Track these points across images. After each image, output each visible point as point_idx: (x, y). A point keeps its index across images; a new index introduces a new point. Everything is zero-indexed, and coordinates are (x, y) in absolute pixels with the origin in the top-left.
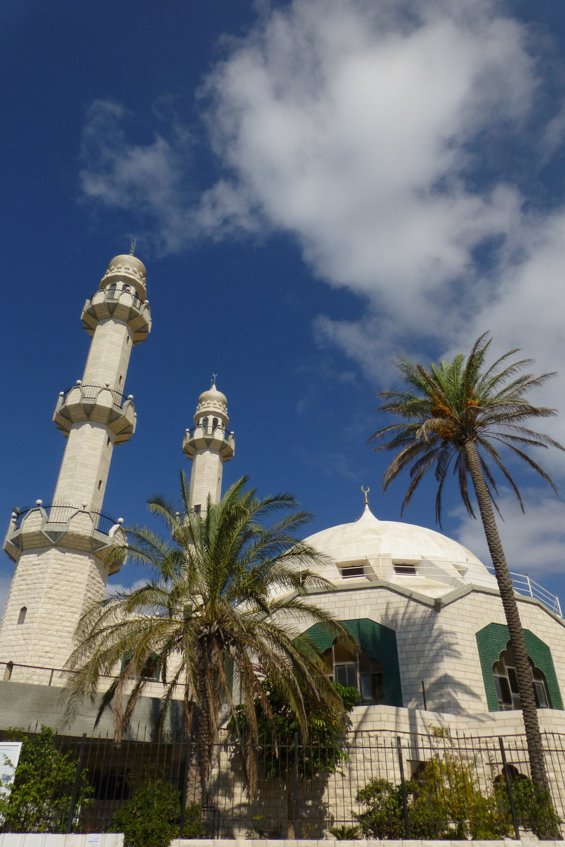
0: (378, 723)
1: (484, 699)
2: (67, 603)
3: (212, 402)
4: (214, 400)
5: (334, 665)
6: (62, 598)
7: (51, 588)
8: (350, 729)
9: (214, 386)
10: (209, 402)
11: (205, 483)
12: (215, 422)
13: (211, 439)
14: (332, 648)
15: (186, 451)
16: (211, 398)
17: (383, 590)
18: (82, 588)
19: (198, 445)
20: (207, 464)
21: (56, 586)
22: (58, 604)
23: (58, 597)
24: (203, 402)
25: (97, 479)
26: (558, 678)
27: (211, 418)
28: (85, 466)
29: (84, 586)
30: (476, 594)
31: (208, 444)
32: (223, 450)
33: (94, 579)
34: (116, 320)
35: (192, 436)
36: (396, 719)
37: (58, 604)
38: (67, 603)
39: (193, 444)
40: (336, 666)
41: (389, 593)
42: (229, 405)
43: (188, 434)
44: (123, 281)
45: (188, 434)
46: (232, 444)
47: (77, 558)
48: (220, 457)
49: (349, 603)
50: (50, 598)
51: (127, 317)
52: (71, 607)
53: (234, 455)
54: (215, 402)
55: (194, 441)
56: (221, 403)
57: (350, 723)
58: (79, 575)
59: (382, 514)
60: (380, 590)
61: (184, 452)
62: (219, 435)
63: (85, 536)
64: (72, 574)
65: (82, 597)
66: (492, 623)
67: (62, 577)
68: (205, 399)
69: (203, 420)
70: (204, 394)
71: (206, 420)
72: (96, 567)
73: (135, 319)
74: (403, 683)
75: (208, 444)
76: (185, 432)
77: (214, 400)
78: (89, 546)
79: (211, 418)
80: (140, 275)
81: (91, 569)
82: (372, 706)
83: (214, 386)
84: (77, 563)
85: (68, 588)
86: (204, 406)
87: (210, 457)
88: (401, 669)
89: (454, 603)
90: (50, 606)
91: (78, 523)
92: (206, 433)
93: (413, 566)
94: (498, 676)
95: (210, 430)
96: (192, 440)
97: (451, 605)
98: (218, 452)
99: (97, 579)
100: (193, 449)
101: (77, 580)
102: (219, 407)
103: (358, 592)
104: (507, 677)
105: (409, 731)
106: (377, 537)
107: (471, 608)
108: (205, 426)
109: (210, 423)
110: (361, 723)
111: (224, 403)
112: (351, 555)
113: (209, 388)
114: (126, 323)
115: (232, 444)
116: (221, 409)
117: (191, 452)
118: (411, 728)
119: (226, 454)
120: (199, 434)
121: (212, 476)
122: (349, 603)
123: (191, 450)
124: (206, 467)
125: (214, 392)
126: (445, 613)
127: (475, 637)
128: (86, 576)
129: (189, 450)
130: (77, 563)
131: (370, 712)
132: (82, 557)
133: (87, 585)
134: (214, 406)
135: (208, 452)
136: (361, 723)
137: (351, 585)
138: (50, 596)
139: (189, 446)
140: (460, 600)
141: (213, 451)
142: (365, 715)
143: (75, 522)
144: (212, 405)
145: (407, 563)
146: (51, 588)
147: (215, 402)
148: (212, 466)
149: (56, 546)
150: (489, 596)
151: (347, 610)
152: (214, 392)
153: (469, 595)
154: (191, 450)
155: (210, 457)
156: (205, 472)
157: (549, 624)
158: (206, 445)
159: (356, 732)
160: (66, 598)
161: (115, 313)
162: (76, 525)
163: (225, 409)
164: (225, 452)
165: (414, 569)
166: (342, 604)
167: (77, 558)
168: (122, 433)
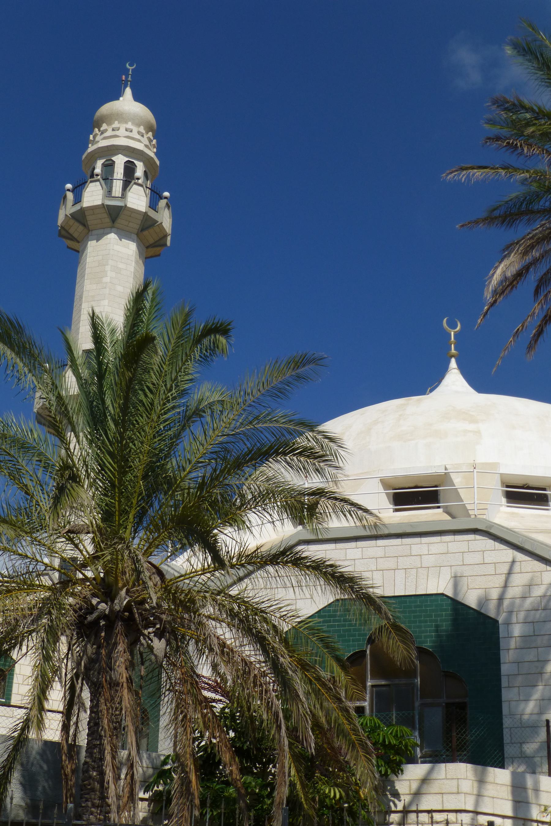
0: (453, 796)
3: (123, 127)
4: (126, 122)
5: (369, 684)
8: (396, 805)
9: (128, 91)
10: (116, 124)
11: (106, 302)
12: (129, 169)
13: (121, 207)
14: (366, 651)
15: (64, 233)
16: (121, 117)
17: (478, 537)
19: (91, 220)
20: (110, 262)
24: (104, 126)
27: (120, 161)
31: (114, 217)
32: (146, 233)
35: (78, 199)
39: (80, 216)
40: (373, 686)
41: (490, 543)
42: (161, 132)
43: (70, 196)
45: (70, 196)
46: (165, 218)
48: (138, 246)
49: (404, 562)
53: (168, 244)
54: (130, 125)
55: (82, 211)
56: (142, 129)
57: (396, 795)
59: (481, 382)
60: (471, 537)
61: (60, 235)
62: (138, 199)
68: (108, 119)
69: (104, 165)
70: (107, 108)
71: (109, 166)
74: (507, 722)
75: (114, 217)
76: (65, 191)
77: (126, 122)
79: (120, 161)
82: (443, 765)
83: (128, 91)
86: (106, 135)
87: (117, 248)
88: (506, 695)
92: (109, 193)
93: (544, 489)
95: (117, 187)
96: (77, 207)
98: (135, 237)
100: (81, 228)
102: (138, 137)
103: (425, 540)
105: (510, 813)
106: (471, 427)
108: (107, 178)
109: (119, 171)
110: (417, 794)
111: (149, 128)
112: (415, 463)
113: (117, 95)
115: (165, 218)
116: (143, 143)
117: (76, 235)
118: (516, 808)
119: (151, 241)
120: (93, 195)
121: (120, 288)
122: (404, 562)
123: (76, 229)
124: (108, 268)
125: (127, 104)
129: (71, 231)
131: (434, 775)
134: (128, 134)
135: (112, 236)
136: (417, 794)
137: (411, 525)
139: (72, 222)
141: (123, 234)
142: (425, 780)
144: (122, 132)
145: (531, 484)
147: (130, 125)
148: (121, 266)
151: (400, 575)
152: (127, 104)
154: (76, 229)
155: (117, 248)
156: (107, 280)
158: (108, 220)
159: (405, 812)
163: (150, 141)
164: (151, 236)
165: (546, 496)
166: (390, 563)
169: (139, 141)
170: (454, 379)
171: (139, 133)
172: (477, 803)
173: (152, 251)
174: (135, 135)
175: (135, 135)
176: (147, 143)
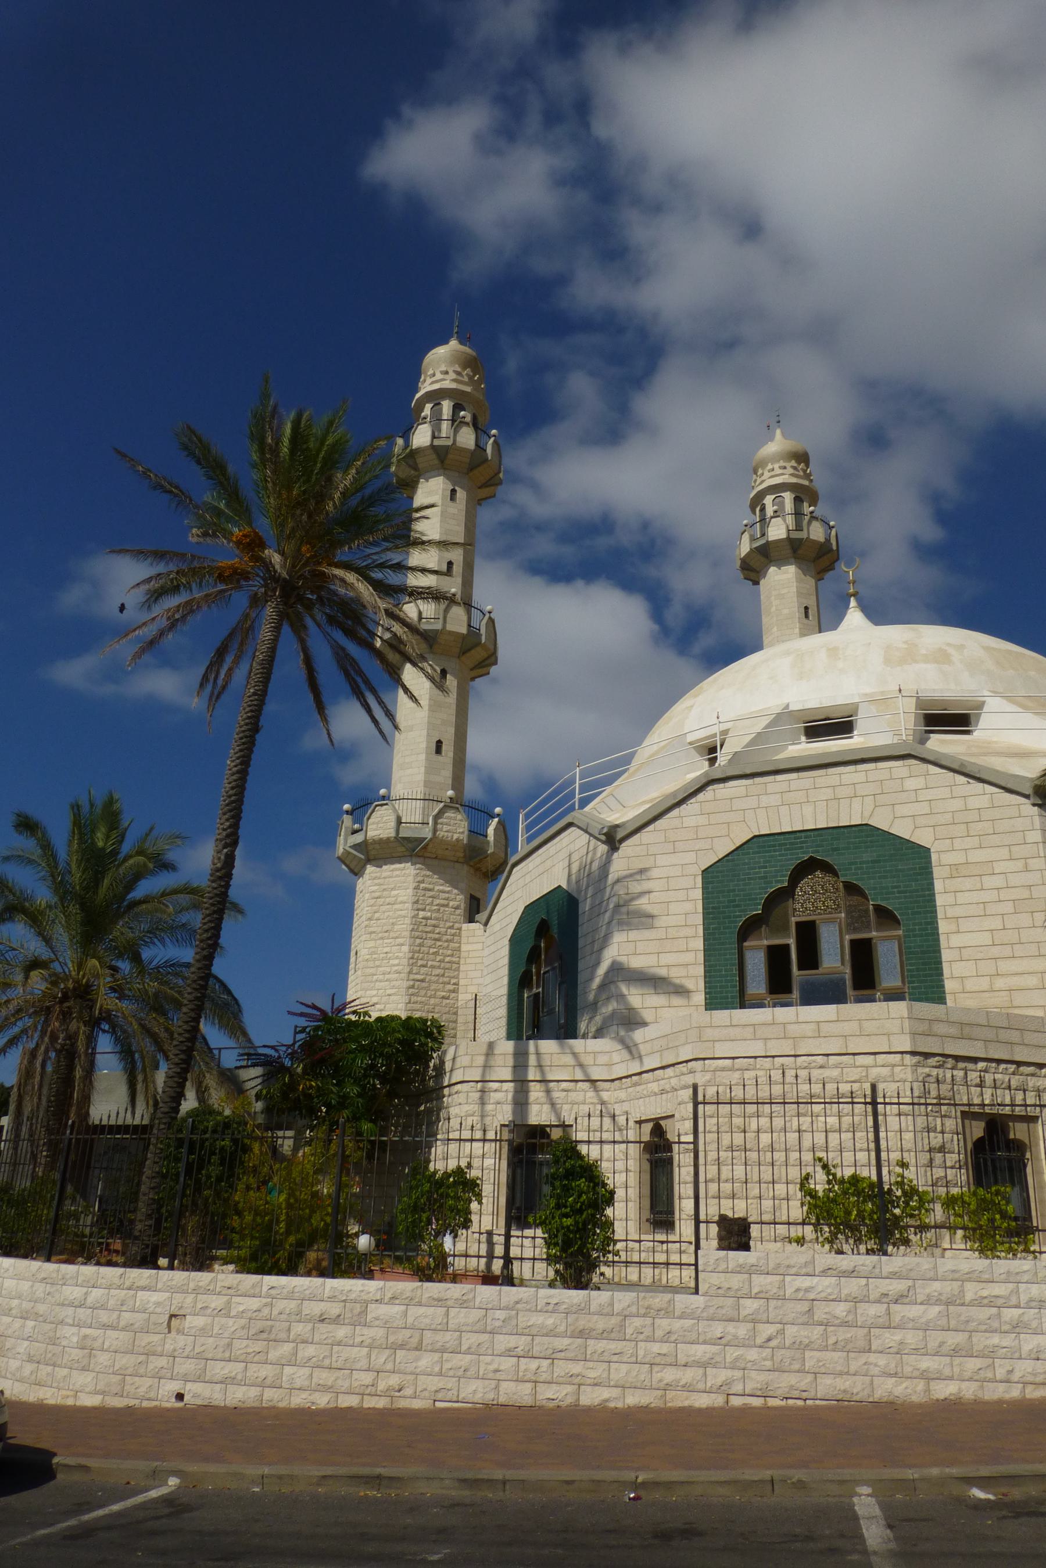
1: (699, 998)
2: (392, 934)
6: (385, 928)
7: (370, 919)
11: (775, 629)
18: (407, 909)
20: (774, 593)
21: (377, 915)
22: (382, 938)
23: (380, 929)
25: (428, 742)
26: (940, 914)
28: (411, 728)
29: (409, 906)
30: (722, 785)
32: (800, 552)
33: (430, 890)
34: (428, 475)
36: (486, 1061)
37: (382, 938)
38: (392, 934)
44: (428, 402)
47: (396, 869)
50: (371, 933)
51: (436, 462)
52: (397, 938)
54: (770, 466)
58: (401, 892)
63: (388, 838)
64: (394, 893)
65: (408, 921)
66: (755, 837)
67: (380, 901)
72: (428, 873)
73: (450, 456)
78: (403, 849)
80: (455, 371)
81: (420, 879)
84: (397, 876)
85: (390, 914)
89: (658, 823)
90: (371, 944)
91: (378, 823)
94: (766, 942)
97: (651, 828)
99: (437, 888)
101: (400, 899)
102: (781, 471)
104: (792, 942)
107: (702, 820)
114: (441, 471)
121: (786, 611)
126: (627, 848)
127: (699, 879)
128: (410, 891)
130: (397, 876)
132: (402, 865)
133: (417, 902)
135: (772, 569)
138: (371, 929)
140: (675, 812)
141: (780, 562)
143: (373, 823)
146: (370, 919)
149: (369, 861)
150: (758, 780)
153: (701, 796)
156: (773, 609)
157: (945, 792)
158: (763, 559)
160: (389, 928)
161: (420, 466)
162: (374, 826)
163: (795, 468)
167: (396, 869)
168: (464, 652)
169: (783, 474)
170: (854, 617)
171: (780, 467)
172: (483, 1075)
173: (825, 561)
174: (778, 471)
175: (778, 471)
176: (792, 471)
